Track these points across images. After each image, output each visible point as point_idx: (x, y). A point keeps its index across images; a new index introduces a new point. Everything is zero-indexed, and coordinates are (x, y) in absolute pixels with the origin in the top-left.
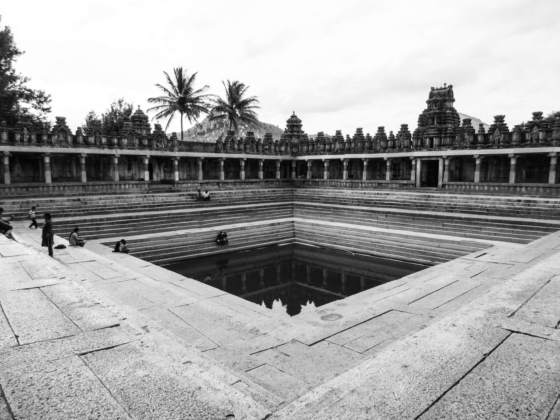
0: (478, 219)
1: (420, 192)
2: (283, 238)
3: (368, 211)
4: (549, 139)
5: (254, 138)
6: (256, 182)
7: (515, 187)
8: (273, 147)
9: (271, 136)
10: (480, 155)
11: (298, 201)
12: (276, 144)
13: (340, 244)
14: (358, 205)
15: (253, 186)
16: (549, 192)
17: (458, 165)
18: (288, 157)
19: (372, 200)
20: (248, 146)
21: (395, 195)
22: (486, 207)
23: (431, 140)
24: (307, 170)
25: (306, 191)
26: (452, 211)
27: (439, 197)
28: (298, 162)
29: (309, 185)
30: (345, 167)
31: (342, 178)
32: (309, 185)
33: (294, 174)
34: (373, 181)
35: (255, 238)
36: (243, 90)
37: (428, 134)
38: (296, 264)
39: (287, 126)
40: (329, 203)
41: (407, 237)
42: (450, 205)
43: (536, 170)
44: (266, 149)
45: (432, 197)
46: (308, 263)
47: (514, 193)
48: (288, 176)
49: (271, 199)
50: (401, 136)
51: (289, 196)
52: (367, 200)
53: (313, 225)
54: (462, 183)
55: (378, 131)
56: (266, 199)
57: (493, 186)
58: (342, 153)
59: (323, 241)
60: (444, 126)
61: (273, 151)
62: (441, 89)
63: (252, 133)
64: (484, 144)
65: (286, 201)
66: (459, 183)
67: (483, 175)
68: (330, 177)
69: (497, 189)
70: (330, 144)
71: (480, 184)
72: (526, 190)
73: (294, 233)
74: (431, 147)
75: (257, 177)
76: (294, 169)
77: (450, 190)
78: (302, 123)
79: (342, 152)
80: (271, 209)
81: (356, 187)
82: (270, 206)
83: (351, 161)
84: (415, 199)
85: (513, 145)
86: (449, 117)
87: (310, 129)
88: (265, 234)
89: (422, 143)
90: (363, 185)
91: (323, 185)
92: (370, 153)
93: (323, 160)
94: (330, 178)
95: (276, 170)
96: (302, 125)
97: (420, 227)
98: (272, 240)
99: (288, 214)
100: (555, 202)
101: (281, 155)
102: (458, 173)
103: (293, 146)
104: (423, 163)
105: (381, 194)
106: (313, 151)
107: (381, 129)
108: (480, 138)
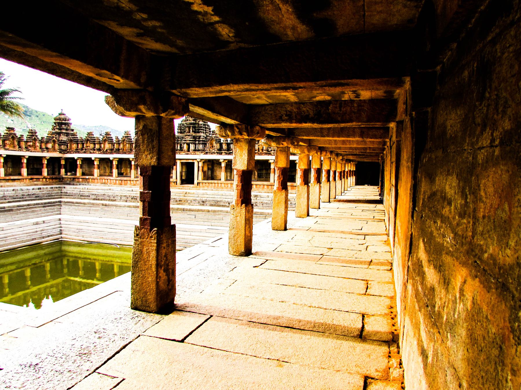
0: (221, 211)
2: (49, 236)
4: (270, 150)
5: (15, 134)
6: (19, 179)
8: (38, 144)
9: (36, 133)
10: (225, 160)
11: (67, 198)
12: (41, 142)
13: (106, 239)
15: (15, 183)
17: (210, 167)
18: (56, 155)
20: (7, 142)
23: (188, 145)
24: (77, 167)
25: (76, 188)
26: (203, 205)
28: (67, 159)
29: (79, 182)
30: (115, 166)
31: (112, 176)
32: (79, 182)
33: (63, 171)
35: (15, 238)
36: (3, 79)
37: (186, 141)
38: (68, 260)
39: (55, 123)
40: (99, 199)
43: (264, 172)
44: (30, 146)
46: (80, 258)
48: (57, 173)
49: (36, 197)
51: (58, 193)
54: (213, 181)
56: (30, 197)
58: (111, 153)
60: (198, 134)
61: (38, 148)
63: (13, 129)
65: (54, 198)
66: (210, 181)
67: (229, 175)
68: (101, 175)
70: (100, 143)
72: (256, 187)
73: (61, 230)
75: (20, 174)
76: (63, 166)
77: (203, 187)
78: (70, 122)
79: (112, 151)
80: (36, 207)
81: (125, 184)
82: (34, 204)
83: (121, 161)
86: (201, 127)
87: (80, 127)
88: (27, 233)
89: (181, 148)
90: (132, 182)
91: (94, 182)
93: (93, 159)
94: (101, 175)
95: (43, 167)
96: (71, 124)
98: (35, 239)
99: (55, 211)
101: (48, 152)
102: (210, 173)
103: (61, 143)
104: (182, 164)
106: (82, 149)
108: (225, 147)
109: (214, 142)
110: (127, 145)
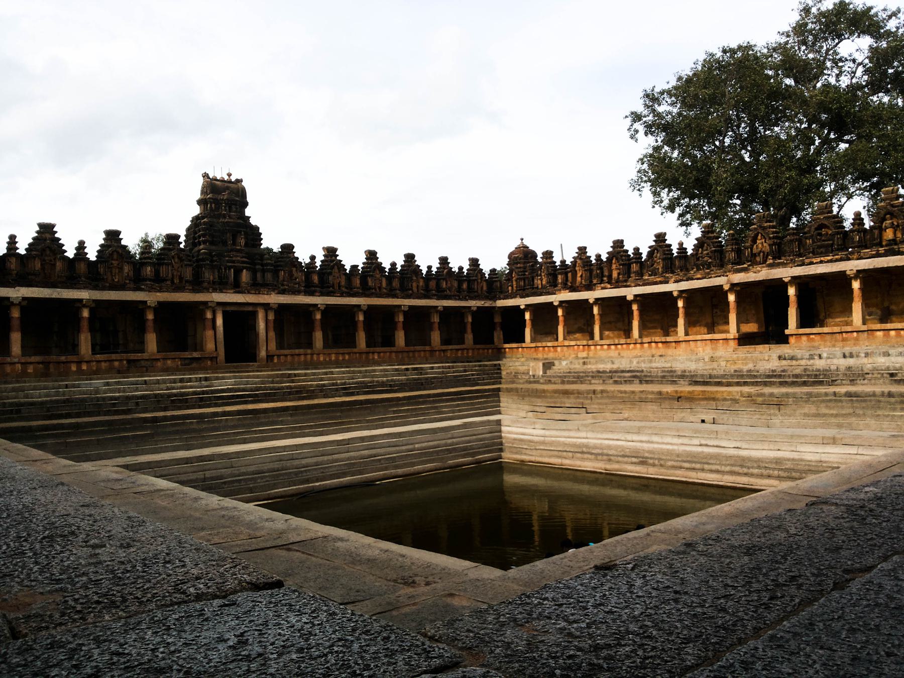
1: (234, 372)
3: (239, 413)
7: (368, 353)
13: (317, 481)
14: (165, 409)
16: (403, 357)
19: (182, 394)
21: (223, 378)
22: (383, 382)
26: (352, 394)
27: (306, 375)
30: (16, 323)
34: (114, 356)
37: (233, 262)
41: (400, 435)
42: (336, 384)
45: (295, 375)
47: (368, 363)
50: (173, 257)
52: (170, 395)
53: (187, 461)
54: (302, 351)
55: (104, 239)
57: (343, 354)
59: (275, 486)
62: (223, 181)
64: (322, 287)
66: (297, 351)
69: (347, 357)
71: (326, 351)
72: (379, 357)
74: (237, 287)
81: (66, 374)
84: (273, 382)
85: (358, 293)
89: (220, 277)
92: (95, 288)
97: (368, 421)
100: (439, 368)
105: (190, 380)
107: (113, 236)
109: (294, 269)
110: (59, 265)
